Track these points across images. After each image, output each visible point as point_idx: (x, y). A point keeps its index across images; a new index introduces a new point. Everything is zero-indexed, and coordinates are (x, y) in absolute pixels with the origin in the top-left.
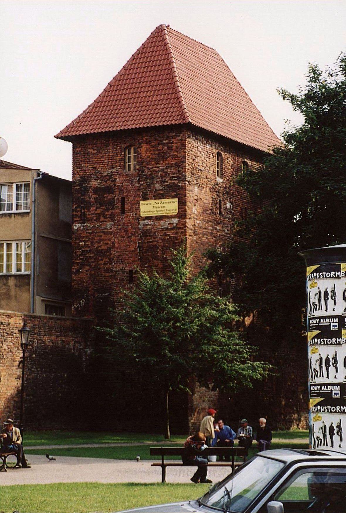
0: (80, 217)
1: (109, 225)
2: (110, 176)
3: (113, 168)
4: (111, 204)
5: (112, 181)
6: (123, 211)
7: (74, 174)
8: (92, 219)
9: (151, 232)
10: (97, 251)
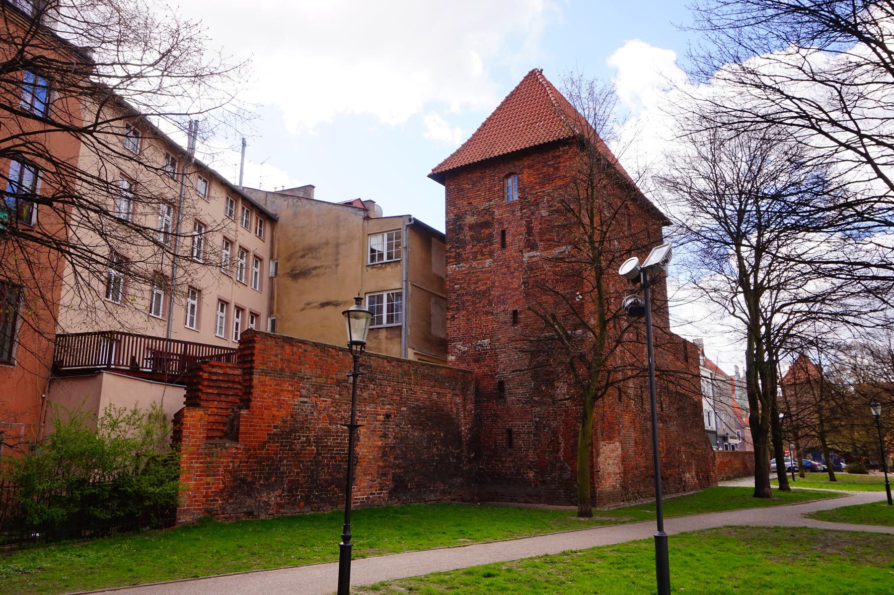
0: (455, 258)
1: (488, 262)
2: (488, 211)
3: (491, 201)
4: (490, 239)
5: (490, 215)
6: (503, 245)
7: (447, 213)
8: (468, 258)
9: (538, 264)
10: (475, 293)
